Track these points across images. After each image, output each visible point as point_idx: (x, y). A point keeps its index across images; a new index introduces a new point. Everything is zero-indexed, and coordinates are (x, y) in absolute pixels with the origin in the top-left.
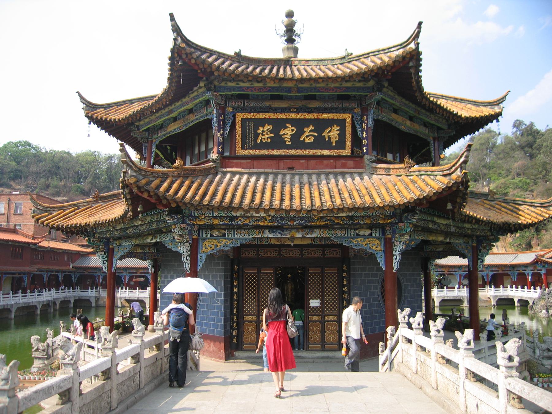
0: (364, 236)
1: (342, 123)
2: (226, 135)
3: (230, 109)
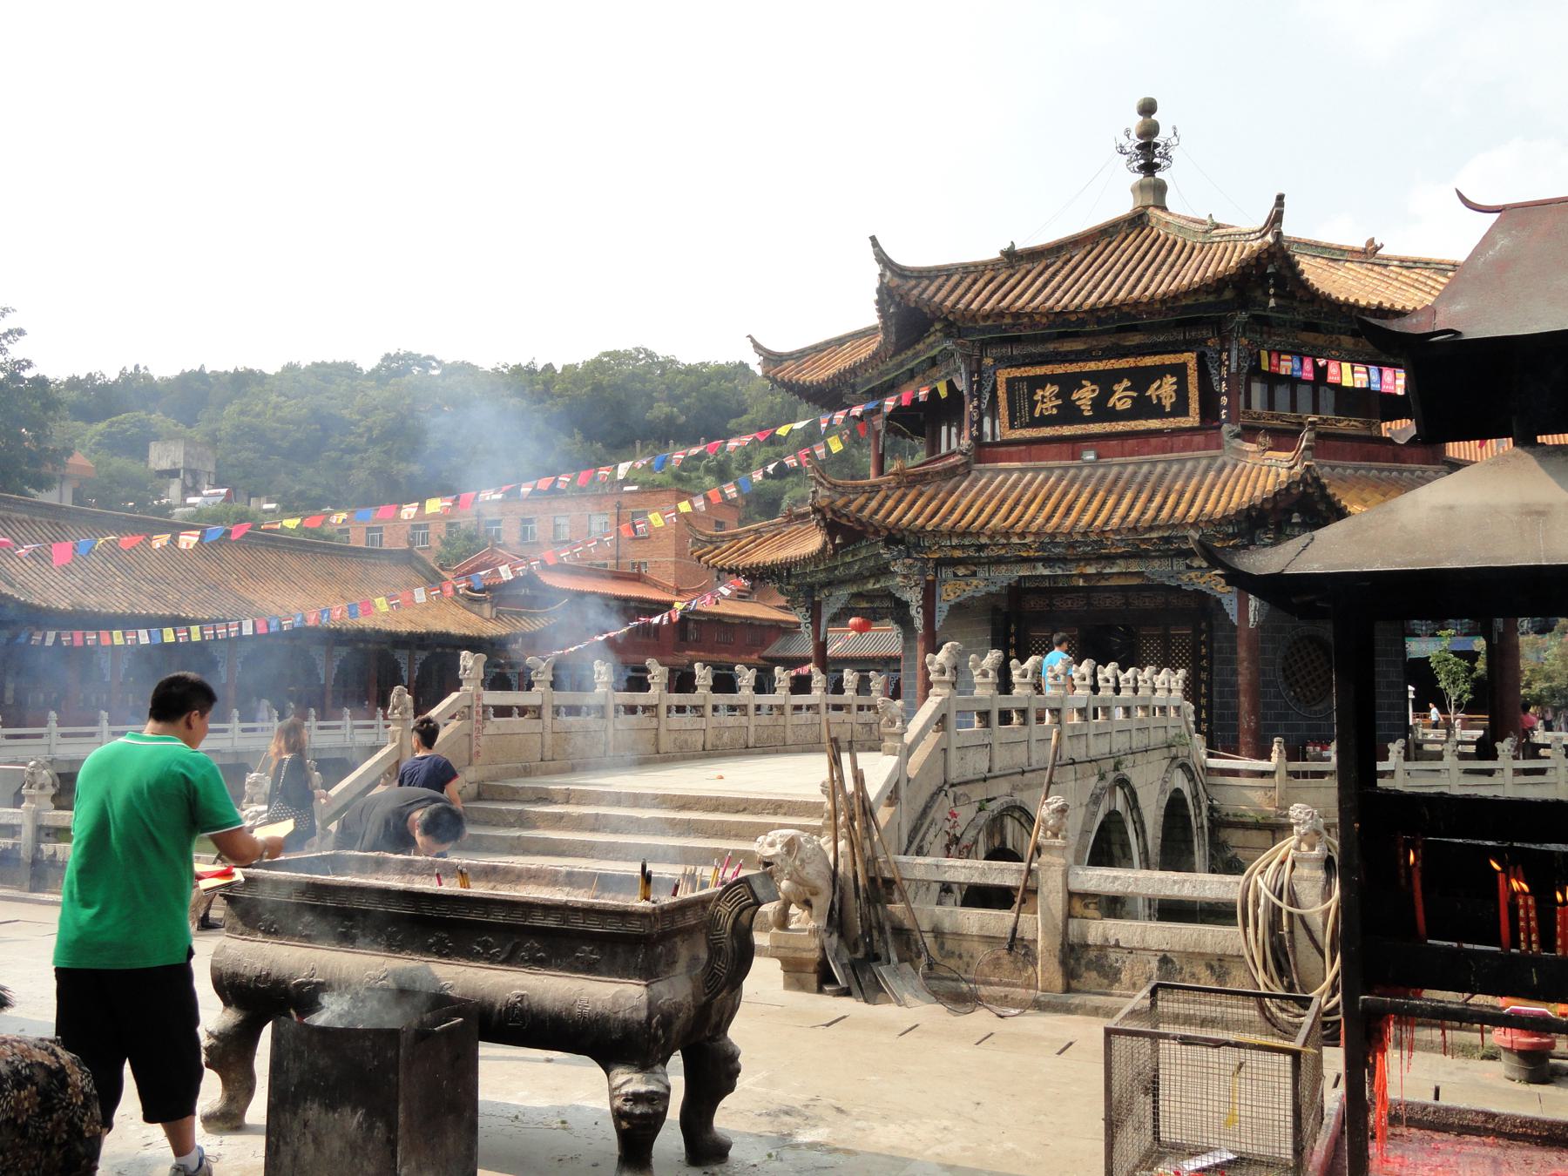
0: (1200, 568)
1: (1179, 371)
2: (983, 407)
3: (988, 361)
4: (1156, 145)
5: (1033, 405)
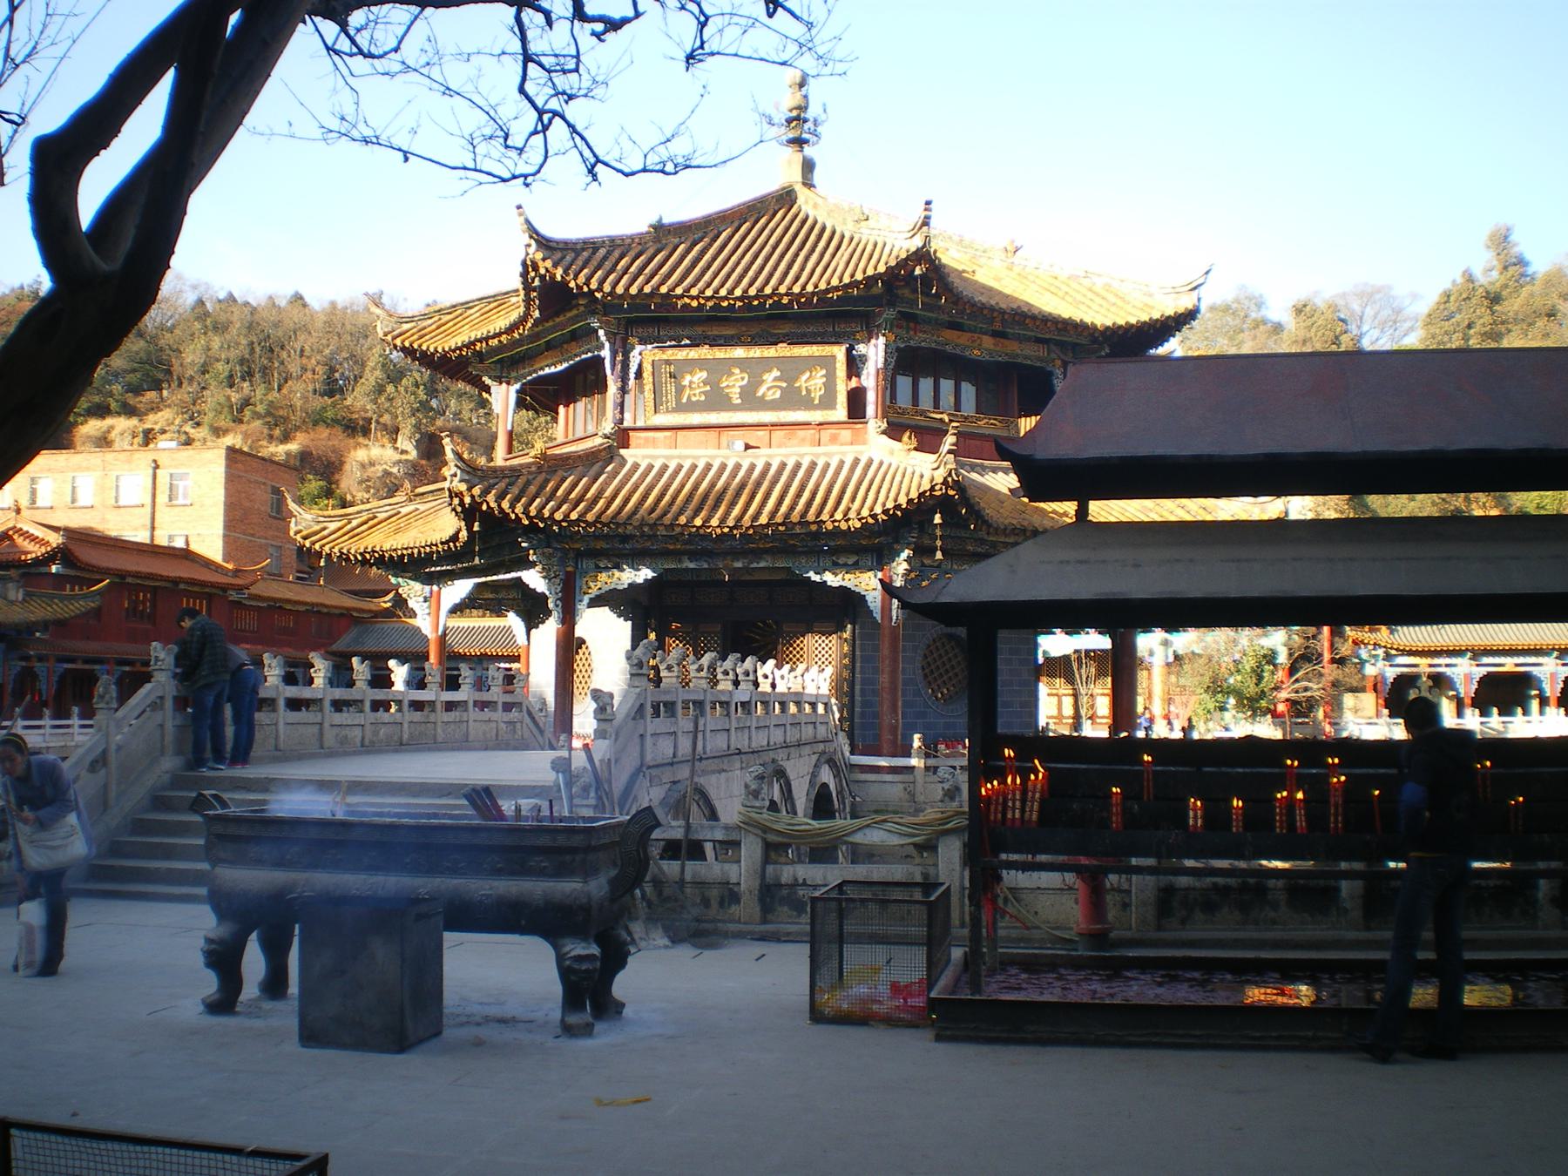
4: (805, 121)
5: (680, 390)
